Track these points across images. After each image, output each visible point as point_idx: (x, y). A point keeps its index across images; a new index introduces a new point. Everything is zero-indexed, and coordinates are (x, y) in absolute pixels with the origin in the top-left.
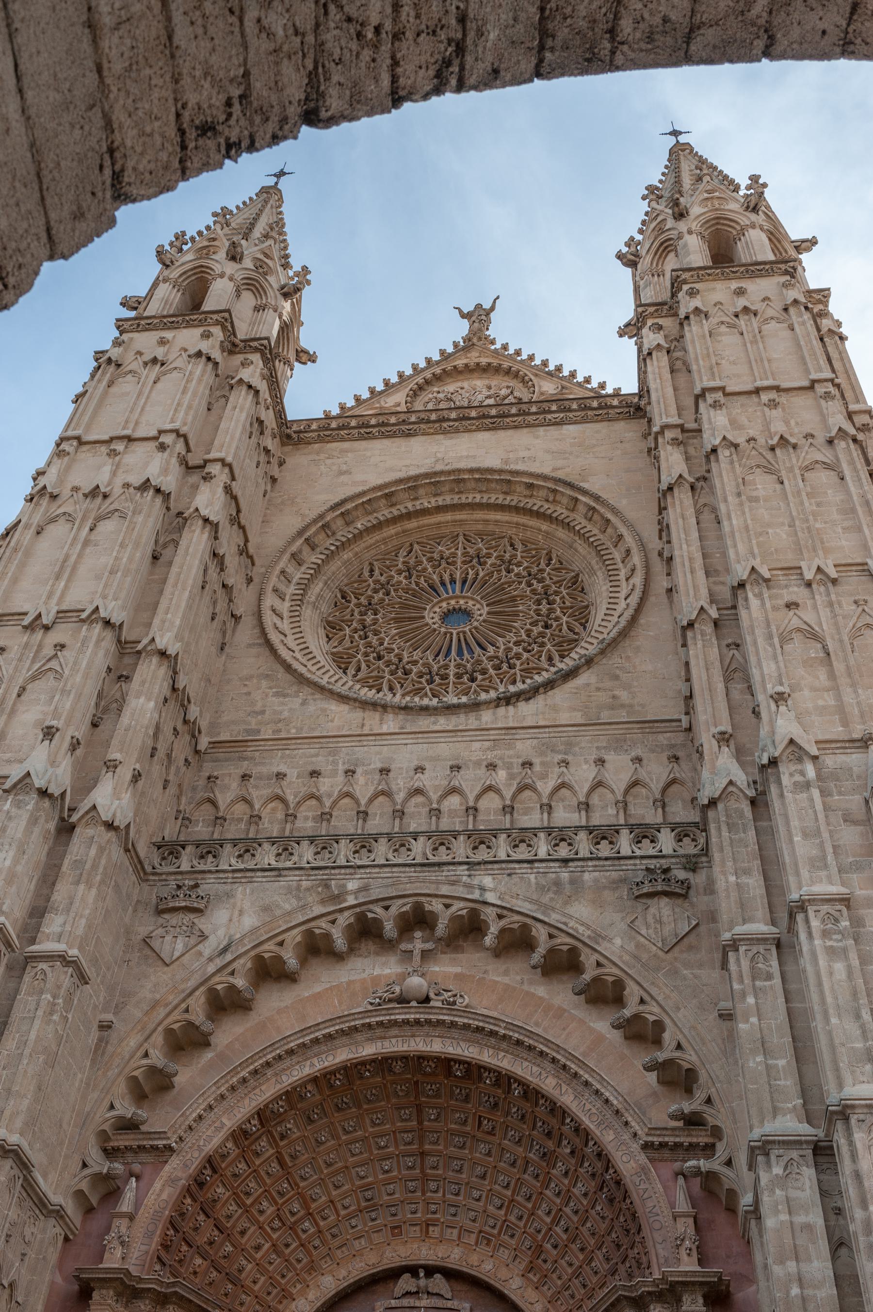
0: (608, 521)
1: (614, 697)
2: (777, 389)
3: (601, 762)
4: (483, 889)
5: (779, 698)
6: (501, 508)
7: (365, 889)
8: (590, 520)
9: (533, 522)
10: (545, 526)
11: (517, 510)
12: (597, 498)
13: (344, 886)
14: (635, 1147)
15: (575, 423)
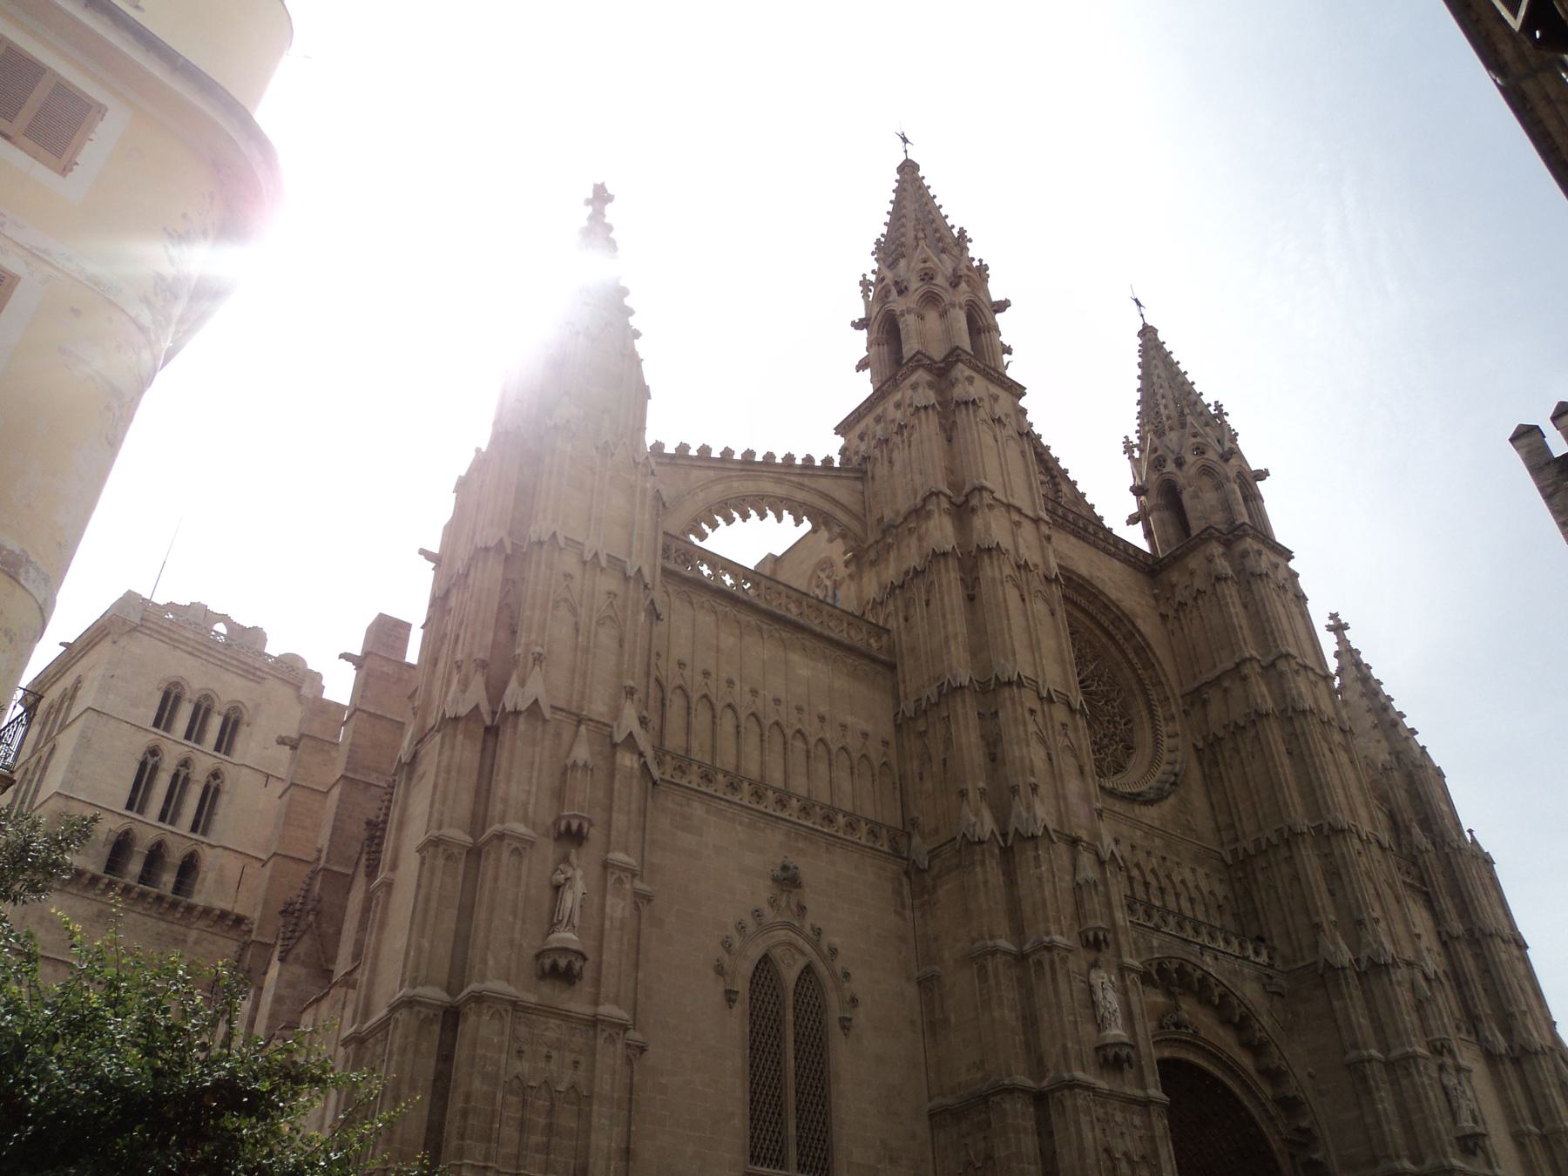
0: (1153, 665)
1: (1188, 821)
2: (1312, 669)
3: (1193, 870)
4: (1208, 965)
5: (1377, 921)
6: (1083, 610)
7: (1160, 946)
8: (1137, 654)
9: (1097, 632)
10: (1104, 640)
11: (1093, 618)
12: (1148, 645)
13: (1151, 942)
14: (1277, 1137)
15: (1119, 560)
